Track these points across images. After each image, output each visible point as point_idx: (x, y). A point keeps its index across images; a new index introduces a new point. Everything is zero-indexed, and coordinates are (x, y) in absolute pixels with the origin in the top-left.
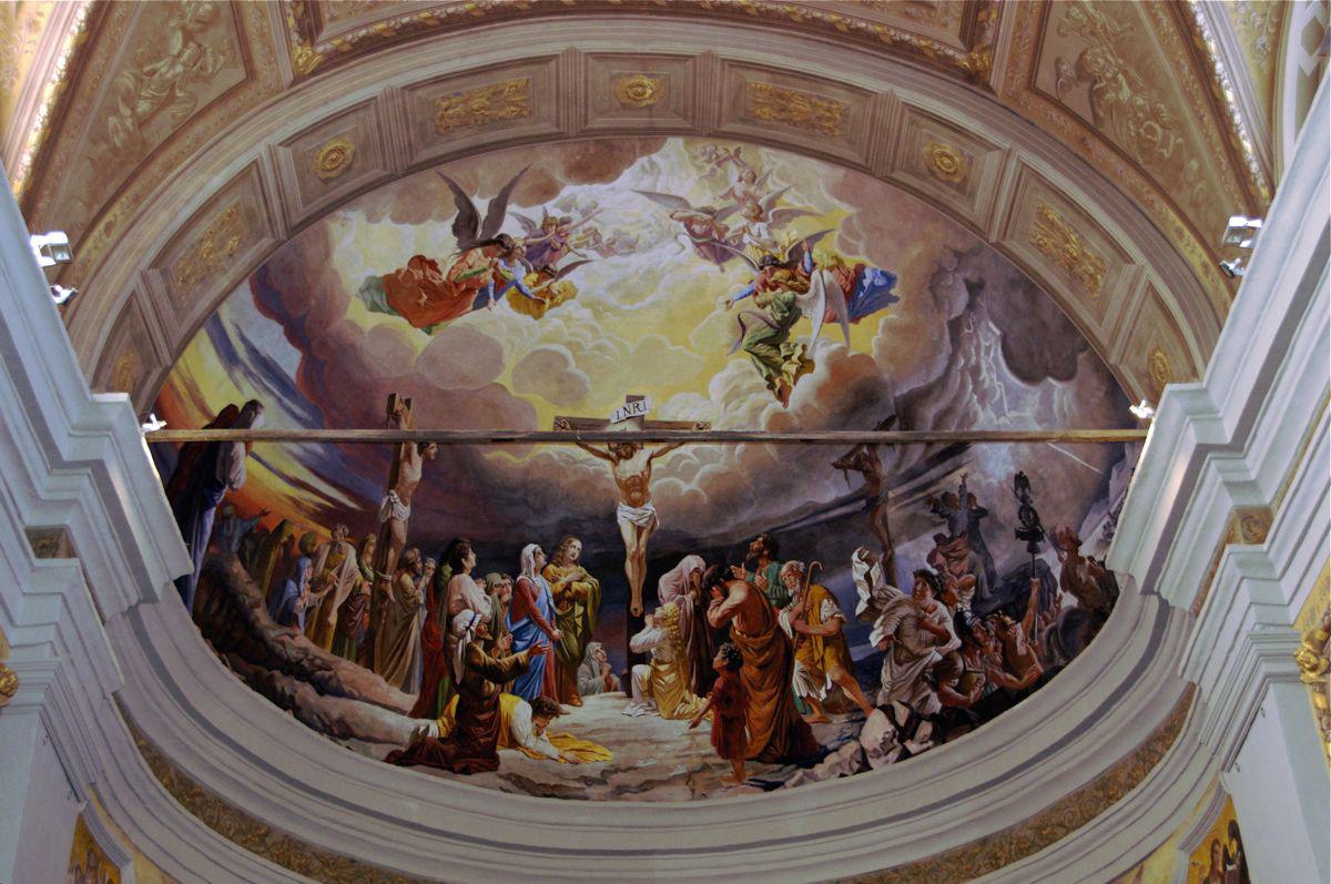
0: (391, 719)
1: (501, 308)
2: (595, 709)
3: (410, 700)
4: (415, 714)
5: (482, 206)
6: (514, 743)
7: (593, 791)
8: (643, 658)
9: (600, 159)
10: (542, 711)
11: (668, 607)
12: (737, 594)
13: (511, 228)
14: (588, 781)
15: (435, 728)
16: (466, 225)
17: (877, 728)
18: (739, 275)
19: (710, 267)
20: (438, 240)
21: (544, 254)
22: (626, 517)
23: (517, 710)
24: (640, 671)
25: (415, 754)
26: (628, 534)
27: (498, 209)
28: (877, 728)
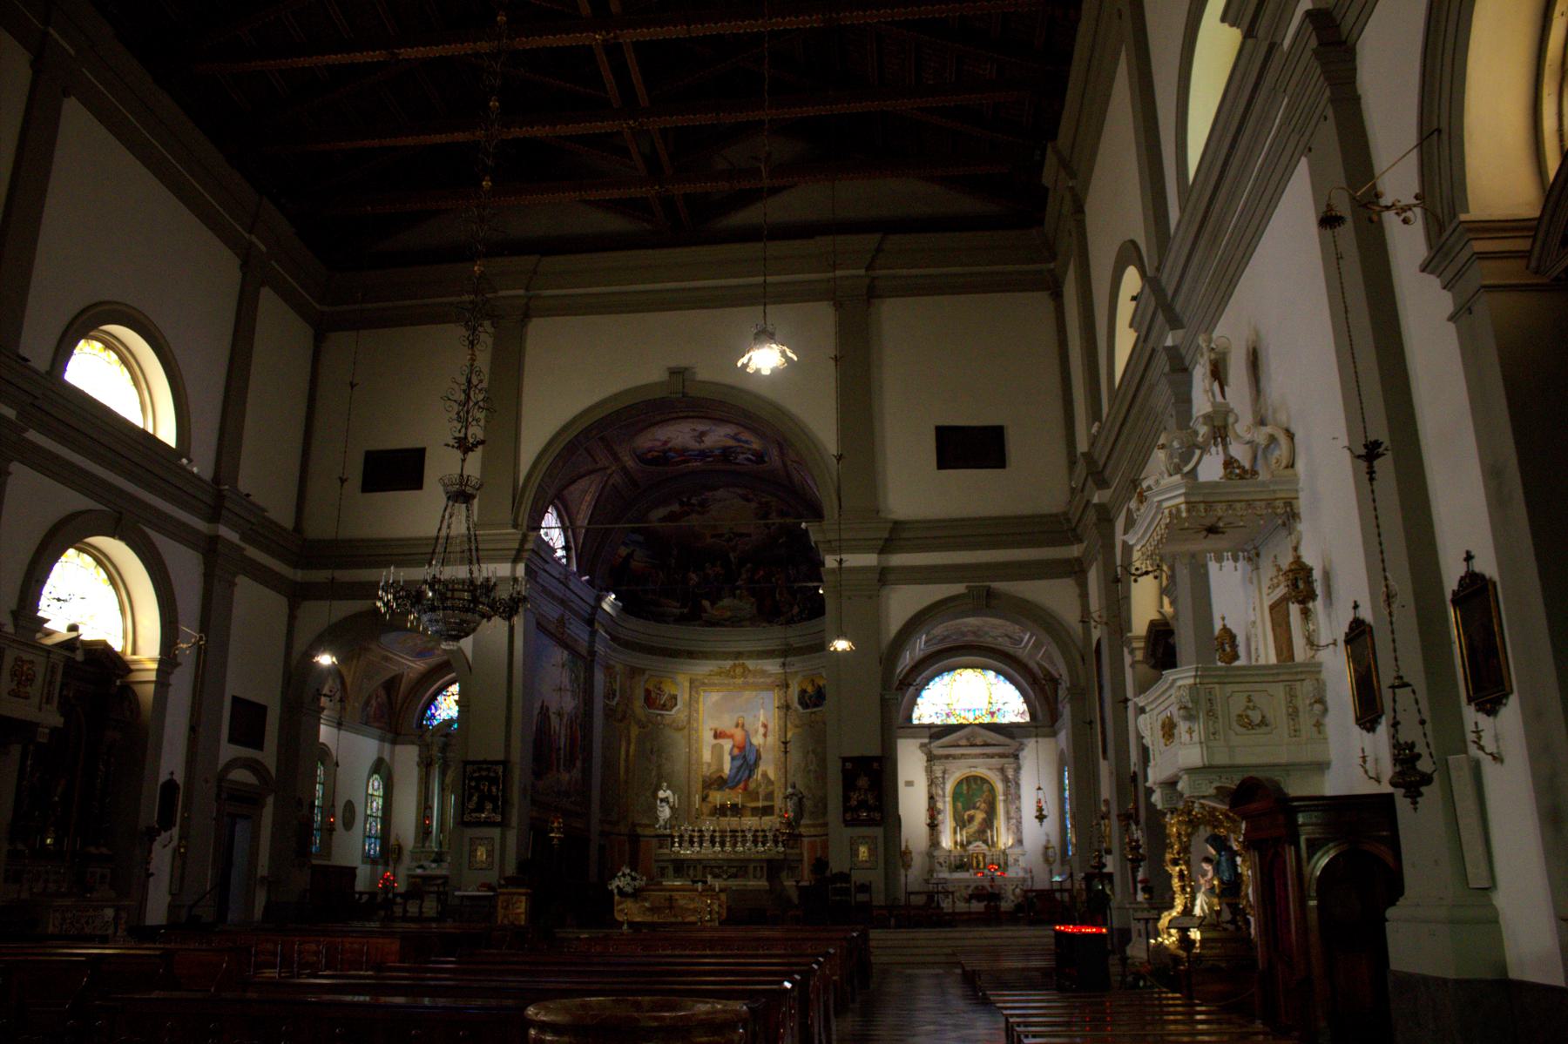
0: (675, 610)
1: (694, 516)
2: (726, 602)
3: (678, 605)
4: (681, 607)
5: (685, 499)
6: (706, 612)
7: (728, 623)
8: (739, 588)
9: (716, 489)
10: (713, 604)
11: (744, 576)
12: (762, 573)
13: (693, 501)
14: (726, 620)
15: (685, 611)
16: (682, 504)
17: (796, 610)
18: (754, 505)
19: (745, 503)
20: (676, 508)
21: (703, 504)
22: (731, 555)
23: (706, 603)
24: (738, 592)
25: (680, 620)
26: (733, 559)
27: (689, 499)
28: (796, 610)
